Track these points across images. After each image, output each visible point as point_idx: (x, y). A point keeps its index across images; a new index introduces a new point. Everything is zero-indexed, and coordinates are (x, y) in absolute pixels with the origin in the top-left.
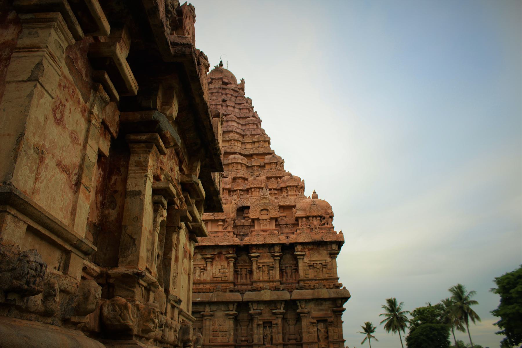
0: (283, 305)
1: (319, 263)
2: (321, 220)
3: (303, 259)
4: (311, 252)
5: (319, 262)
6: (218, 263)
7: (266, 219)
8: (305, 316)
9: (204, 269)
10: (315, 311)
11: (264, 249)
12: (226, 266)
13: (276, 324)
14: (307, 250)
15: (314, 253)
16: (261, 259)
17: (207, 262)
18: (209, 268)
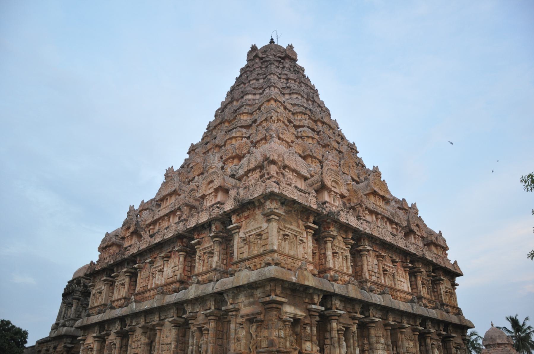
0: (212, 303)
1: (255, 234)
2: (260, 172)
3: (239, 232)
4: (248, 220)
5: (254, 233)
6: (172, 261)
7: (211, 193)
8: (233, 315)
9: (161, 271)
10: (245, 306)
11: (206, 232)
12: (177, 262)
13: (208, 330)
14: (243, 219)
15: (250, 220)
16: (202, 247)
17: (165, 262)
18: (165, 269)
